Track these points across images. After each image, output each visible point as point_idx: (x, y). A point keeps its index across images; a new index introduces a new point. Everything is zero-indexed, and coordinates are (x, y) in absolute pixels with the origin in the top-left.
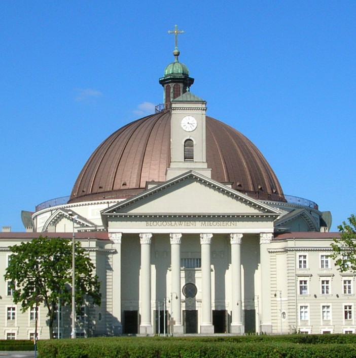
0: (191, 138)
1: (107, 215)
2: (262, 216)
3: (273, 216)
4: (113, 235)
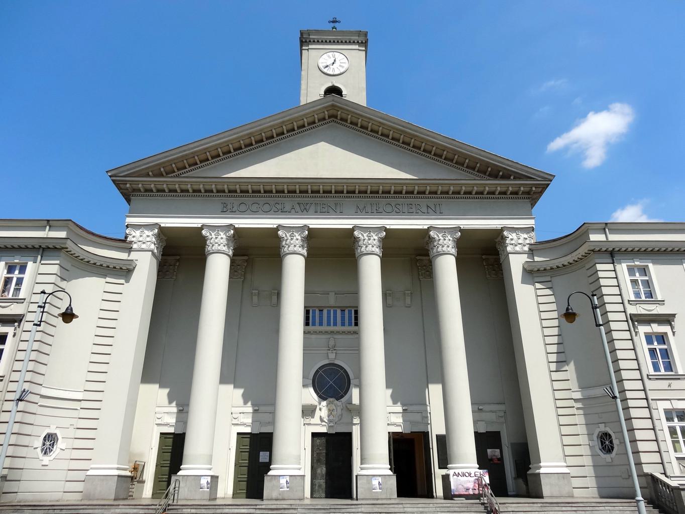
1: (125, 183)
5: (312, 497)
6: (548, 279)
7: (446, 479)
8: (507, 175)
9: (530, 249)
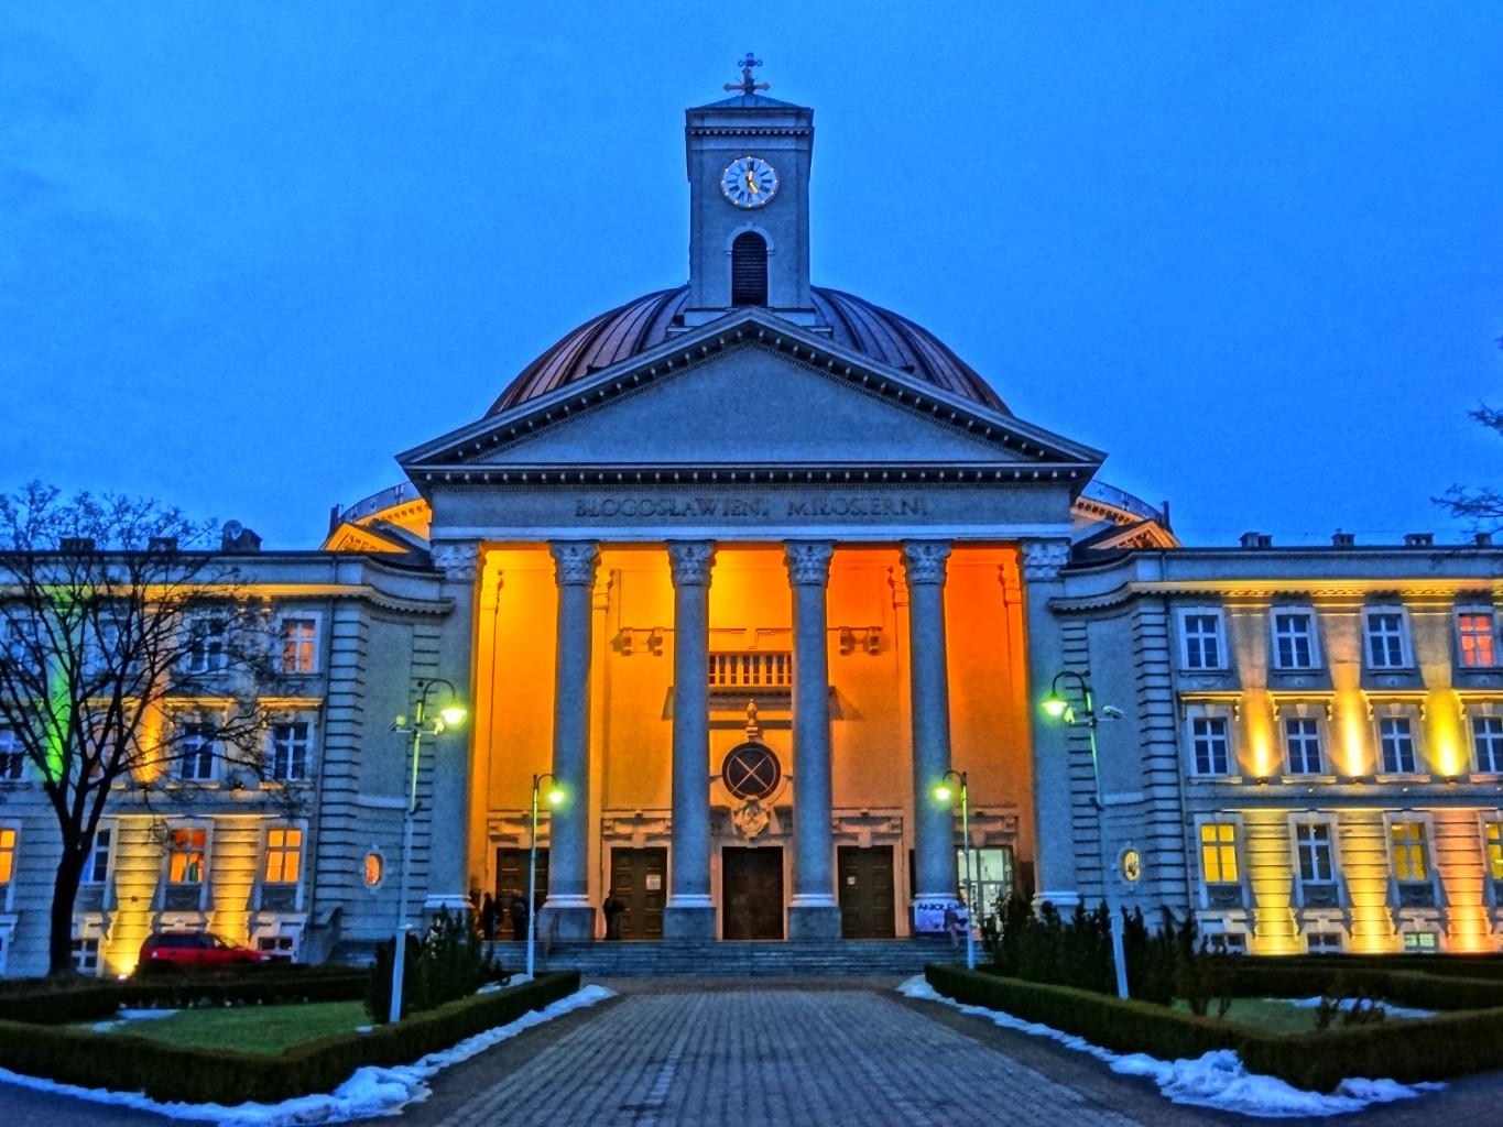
0: (758, 230)
2: (1026, 477)
3: (1064, 476)
4: (449, 552)
5: (725, 936)
6: (1083, 625)
7: (911, 910)
8: (1032, 451)
9: (1059, 574)
